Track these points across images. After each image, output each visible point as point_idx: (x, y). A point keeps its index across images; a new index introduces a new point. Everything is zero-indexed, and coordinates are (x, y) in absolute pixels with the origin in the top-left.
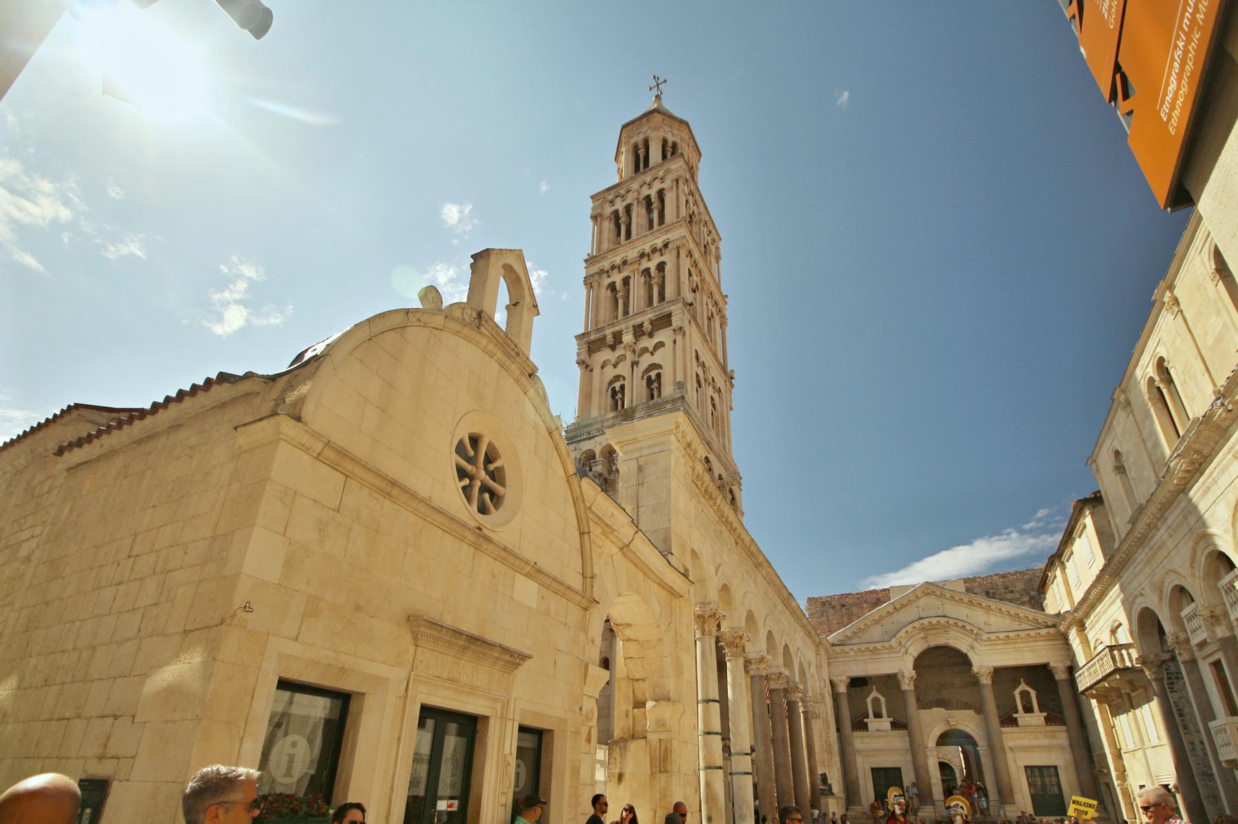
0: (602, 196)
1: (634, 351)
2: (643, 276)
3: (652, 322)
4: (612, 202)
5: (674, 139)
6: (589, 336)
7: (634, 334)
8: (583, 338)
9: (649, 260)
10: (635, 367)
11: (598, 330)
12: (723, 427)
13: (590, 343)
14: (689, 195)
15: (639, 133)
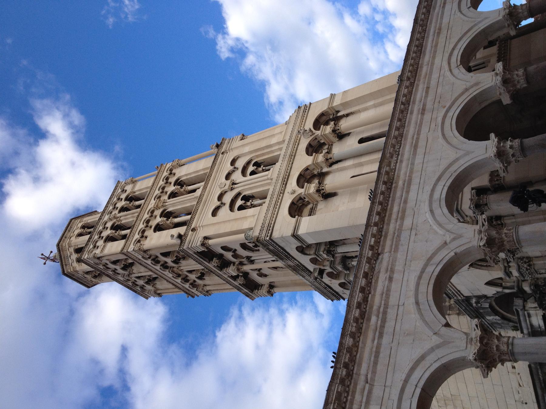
0: (142, 293)
1: (241, 264)
2: (181, 262)
3: (210, 260)
4: (142, 287)
5: (73, 253)
6: (247, 292)
7: (227, 267)
8: (251, 295)
9: (166, 262)
10: (252, 259)
11: (239, 289)
12: (263, 148)
13: (251, 290)
14: (103, 237)
15: (85, 277)
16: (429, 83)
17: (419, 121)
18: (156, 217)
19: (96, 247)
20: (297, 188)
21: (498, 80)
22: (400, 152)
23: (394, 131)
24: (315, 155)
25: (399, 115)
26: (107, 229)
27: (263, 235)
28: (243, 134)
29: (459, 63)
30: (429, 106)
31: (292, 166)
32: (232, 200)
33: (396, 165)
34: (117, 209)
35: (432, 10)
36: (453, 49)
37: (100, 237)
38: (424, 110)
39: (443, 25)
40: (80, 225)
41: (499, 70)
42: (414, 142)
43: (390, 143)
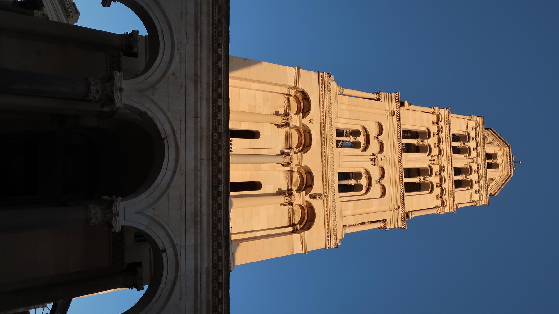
16: (196, 124)
17: (199, 65)
18: (434, 146)
19: (474, 129)
20: (310, 126)
21: (118, 80)
22: (211, 27)
23: (223, 53)
24: (302, 164)
25: (221, 78)
26: (474, 148)
27: (326, 79)
28: (386, 228)
29: (165, 141)
30: (191, 86)
31: (322, 159)
32: (369, 143)
33: (213, 10)
34: (475, 171)
35: (211, 272)
36: (175, 172)
37: (476, 139)
38: (196, 82)
39: (192, 230)
40: (501, 168)
41: (119, 98)
42: (199, 35)
43: (223, 37)
